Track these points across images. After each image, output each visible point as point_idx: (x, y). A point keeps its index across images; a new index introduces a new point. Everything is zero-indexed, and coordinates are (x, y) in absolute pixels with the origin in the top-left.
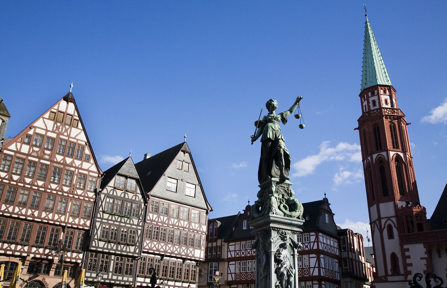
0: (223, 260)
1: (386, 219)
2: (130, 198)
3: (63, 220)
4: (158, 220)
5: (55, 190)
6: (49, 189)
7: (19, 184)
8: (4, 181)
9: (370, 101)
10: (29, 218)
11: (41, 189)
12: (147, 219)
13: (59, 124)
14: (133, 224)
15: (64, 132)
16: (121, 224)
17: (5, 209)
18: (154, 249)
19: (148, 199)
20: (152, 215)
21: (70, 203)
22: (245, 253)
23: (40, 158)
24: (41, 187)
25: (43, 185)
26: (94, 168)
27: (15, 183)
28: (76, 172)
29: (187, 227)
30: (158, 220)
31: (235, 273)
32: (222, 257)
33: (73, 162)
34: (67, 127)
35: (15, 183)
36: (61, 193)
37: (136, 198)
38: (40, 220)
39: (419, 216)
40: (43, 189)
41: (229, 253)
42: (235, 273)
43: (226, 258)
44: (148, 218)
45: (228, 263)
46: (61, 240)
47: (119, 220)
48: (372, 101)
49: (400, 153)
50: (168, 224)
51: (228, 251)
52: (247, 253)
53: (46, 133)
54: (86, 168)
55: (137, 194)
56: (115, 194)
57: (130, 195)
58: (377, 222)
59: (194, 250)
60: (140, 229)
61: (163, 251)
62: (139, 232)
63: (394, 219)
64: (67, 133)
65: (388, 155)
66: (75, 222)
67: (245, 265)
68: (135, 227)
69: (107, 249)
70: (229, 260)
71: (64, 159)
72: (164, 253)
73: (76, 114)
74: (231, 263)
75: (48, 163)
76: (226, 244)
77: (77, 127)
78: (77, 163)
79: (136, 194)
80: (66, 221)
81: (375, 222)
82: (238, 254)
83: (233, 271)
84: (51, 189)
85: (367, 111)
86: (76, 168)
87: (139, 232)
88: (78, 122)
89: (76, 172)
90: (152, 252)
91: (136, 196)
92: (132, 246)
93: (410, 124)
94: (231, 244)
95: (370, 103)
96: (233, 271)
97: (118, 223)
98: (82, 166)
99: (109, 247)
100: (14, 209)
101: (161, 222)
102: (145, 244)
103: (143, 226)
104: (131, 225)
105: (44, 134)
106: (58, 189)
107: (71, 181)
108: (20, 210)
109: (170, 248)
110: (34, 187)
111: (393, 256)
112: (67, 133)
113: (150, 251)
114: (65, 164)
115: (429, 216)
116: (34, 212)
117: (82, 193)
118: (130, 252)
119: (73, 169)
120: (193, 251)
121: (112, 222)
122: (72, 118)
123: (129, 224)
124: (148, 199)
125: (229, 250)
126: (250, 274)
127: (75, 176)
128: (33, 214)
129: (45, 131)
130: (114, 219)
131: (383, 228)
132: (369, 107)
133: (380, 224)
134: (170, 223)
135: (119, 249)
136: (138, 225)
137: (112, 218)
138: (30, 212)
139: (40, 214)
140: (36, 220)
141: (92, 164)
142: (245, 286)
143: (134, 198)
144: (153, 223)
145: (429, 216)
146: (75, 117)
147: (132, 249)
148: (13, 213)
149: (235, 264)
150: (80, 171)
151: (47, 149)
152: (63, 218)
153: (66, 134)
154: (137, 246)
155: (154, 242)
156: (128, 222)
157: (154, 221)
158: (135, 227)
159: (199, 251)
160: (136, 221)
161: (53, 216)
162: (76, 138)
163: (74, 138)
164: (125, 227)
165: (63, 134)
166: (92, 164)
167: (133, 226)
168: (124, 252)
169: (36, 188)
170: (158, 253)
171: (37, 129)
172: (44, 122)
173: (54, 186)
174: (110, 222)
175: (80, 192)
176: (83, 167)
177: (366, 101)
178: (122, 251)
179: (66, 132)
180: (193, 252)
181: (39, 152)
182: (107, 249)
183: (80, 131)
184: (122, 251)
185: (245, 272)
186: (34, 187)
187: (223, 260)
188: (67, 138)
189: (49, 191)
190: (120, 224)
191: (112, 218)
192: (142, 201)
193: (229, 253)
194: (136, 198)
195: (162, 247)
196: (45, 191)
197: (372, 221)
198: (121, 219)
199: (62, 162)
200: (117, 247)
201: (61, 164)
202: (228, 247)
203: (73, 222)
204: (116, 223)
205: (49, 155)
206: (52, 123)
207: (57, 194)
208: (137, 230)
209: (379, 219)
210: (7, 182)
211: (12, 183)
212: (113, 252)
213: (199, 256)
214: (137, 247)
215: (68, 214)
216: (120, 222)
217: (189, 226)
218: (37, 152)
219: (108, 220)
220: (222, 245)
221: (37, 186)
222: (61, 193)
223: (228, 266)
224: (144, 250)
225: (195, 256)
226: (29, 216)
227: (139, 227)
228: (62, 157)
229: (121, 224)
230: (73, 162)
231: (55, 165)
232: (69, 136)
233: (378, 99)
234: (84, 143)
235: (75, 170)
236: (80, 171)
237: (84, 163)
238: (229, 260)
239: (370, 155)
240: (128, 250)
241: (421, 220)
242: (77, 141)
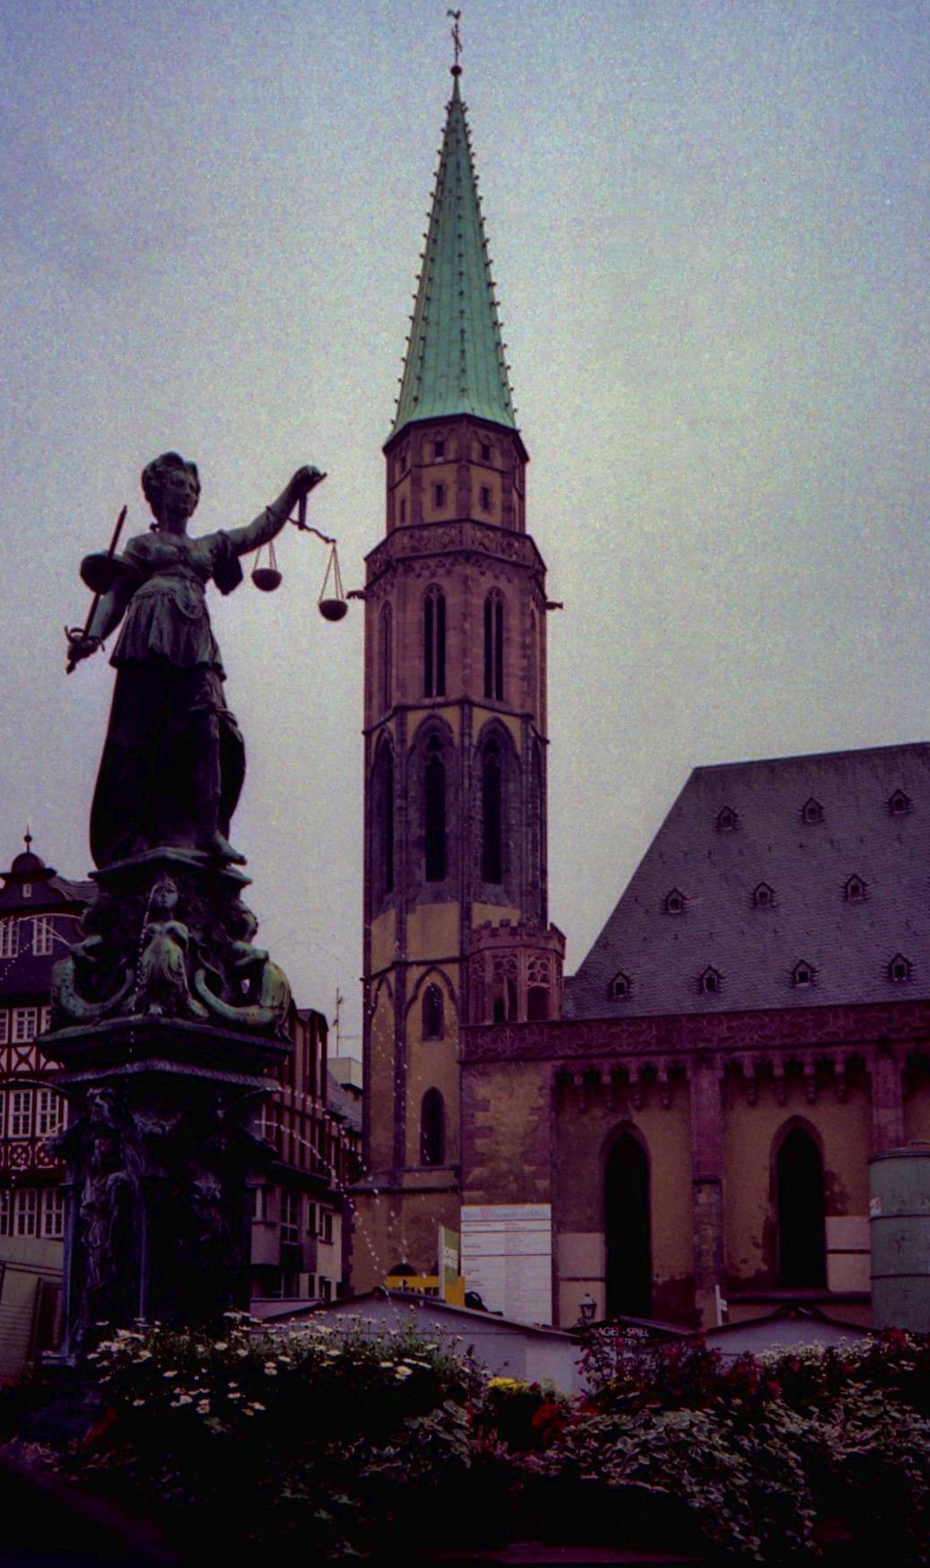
1: (422, 969)
9: (426, 483)
39: (539, 962)
48: (433, 483)
49: (505, 719)
58: (392, 977)
63: (453, 971)
65: (466, 721)
81: (382, 975)
85: (407, 523)
93: (560, 606)
95: (423, 490)
111: (433, 1100)
115: (571, 967)
131: (408, 997)
132: (418, 505)
133: (401, 981)
145: (571, 967)
177: (408, 481)
197: (374, 972)
209: (401, 966)
233: (455, 482)
239: (399, 714)
241: (544, 979)
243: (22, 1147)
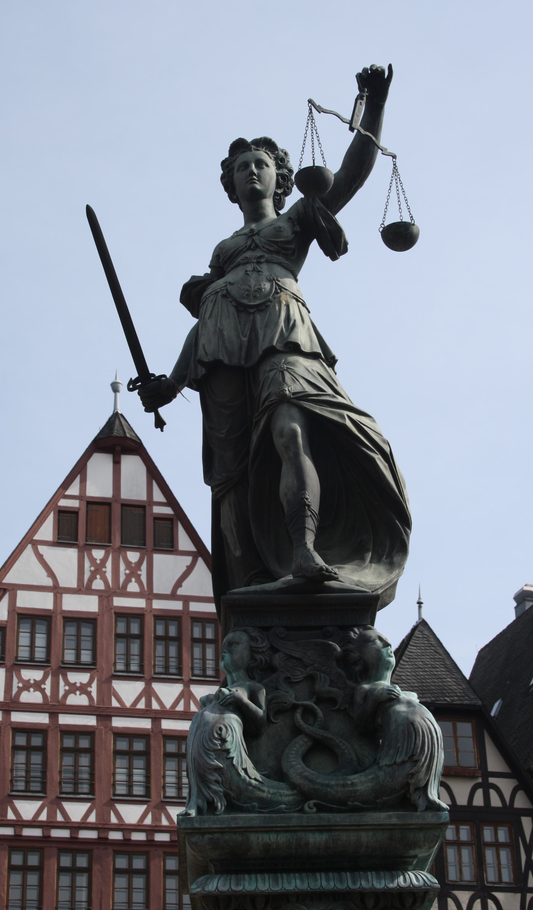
5: (138, 828)
13: (98, 554)
15: (128, 580)
34: (133, 556)
37: (487, 798)
53: (57, 601)
55: (492, 780)
73: (158, 496)
75: (91, 721)
77: (172, 546)
79: (485, 780)
88: (172, 524)
91: (486, 787)
105: (50, 606)
110: (56, 833)
122: (145, 515)
129: (50, 596)
143: (478, 800)
146: (157, 510)
153: (133, 587)
162: (180, 592)
163: (173, 596)
169: (65, 834)
171: (20, 593)
172: (40, 558)
179: (133, 580)
183: (188, 560)
188: (140, 603)
189: (115, 836)
194: (487, 798)
199: (180, 707)
206: (72, 553)
231: (118, 723)
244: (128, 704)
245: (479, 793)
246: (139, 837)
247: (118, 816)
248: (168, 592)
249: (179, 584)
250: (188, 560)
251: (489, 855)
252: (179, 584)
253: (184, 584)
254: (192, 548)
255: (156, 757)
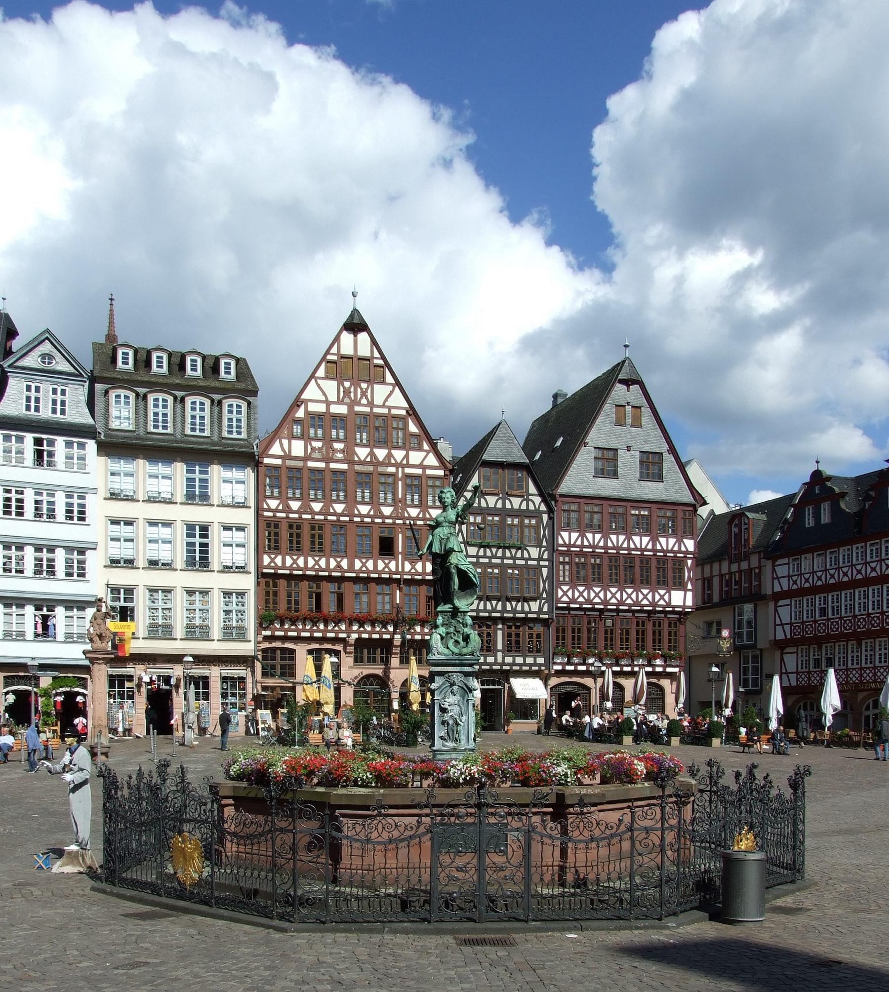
0: (764, 598)
2: (516, 507)
3: (393, 568)
4: (582, 541)
5: (368, 516)
6: (357, 516)
7: (304, 516)
8: (279, 515)
10: (334, 574)
11: (342, 519)
12: (558, 543)
14: (530, 559)
16: (506, 561)
17: (292, 564)
18: (581, 599)
19: (553, 503)
20: (567, 534)
21: (400, 535)
22: (823, 578)
23: (328, 460)
24: (342, 515)
25: (343, 511)
26: (432, 460)
27: (296, 516)
28: (400, 475)
29: (650, 547)
30: (582, 541)
31: (791, 624)
32: (763, 592)
33: (389, 455)
35: (296, 516)
36: (379, 520)
37: (528, 505)
38: (354, 575)
40: (347, 519)
41: (776, 581)
42: (791, 624)
43: (769, 592)
44: (561, 542)
45: (776, 604)
46: (397, 604)
47: (500, 554)
50: (605, 547)
51: (773, 579)
52: (816, 579)
54: (418, 463)
56: (483, 504)
57: (516, 502)
59: (669, 591)
60: (545, 566)
61: (600, 601)
62: (545, 571)
64: (367, 398)
66: (416, 570)
67: (812, 606)
68: (535, 563)
69: (485, 610)
70: (777, 597)
71: (372, 454)
72: (602, 607)
74: (781, 603)
75: (344, 466)
76: (769, 564)
78: (399, 455)
80: (400, 570)
82: (795, 582)
83: (786, 620)
84: (360, 515)
86: (397, 465)
87: (545, 571)
89: (400, 475)
90: (578, 606)
91: (528, 500)
92: (534, 599)
94: (779, 562)
96: (786, 620)
97: (499, 561)
98: (408, 461)
99: (489, 607)
100: (306, 563)
101: (589, 546)
102: (560, 593)
103: (550, 560)
104: (526, 560)
106: (372, 513)
107: (395, 494)
108: (317, 563)
109: (614, 595)
110: (330, 518)
112: (367, 398)
113: (572, 606)
114: (375, 462)
116: (341, 561)
117: (419, 514)
118: (531, 612)
119: (392, 470)
120: (667, 594)
121: (487, 560)
123: (522, 558)
124: (553, 503)
125: (775, 576)
126: (824, 624)
127: (400, 483)
128: (339, 565)
130: (489, 553)
134: (610, 544)
135: (509, 608)
136: (540, 559)
137: (485, 552)
138: (333, 564)
139: (351, 565)
140: (347, 574)
141: (428, 452)
142: (814, 648)
143: (524, 507)
144: (572, 549)
147: (534, 606)
148: (306, 568)
149: (790, 605)
150: (407, 471)
151: (338, 440)
152: (392, 565)
153: (364, 401)
154: (544, 599)
155: (578, 587)
156: (519, 555)
157: (574, 546)
158: (535, 563)
159: (682, 593)
160: (534, 552)
161: (375, 565)
162: (387, 404)
163: (383, 406)
164: (514, 566)
165: (359, 404)
166: (428, 452)
167: (530, 562)
168: (519, 612)
169: (334, 518)
170: (590, 606)
173: (364, 509)
174: (481, 560)
175: (414, 512)
176: (411, 462)
178: (514, 611)
180: (666, 597)
181: (324, 450)
182: (485, 610)
183: (391, 388)
184: (514, 611)
185: (813, 619)
186: (330, 518)
187: (764, 598)
188: (368, 409)
190: (502, 561)
191: (485, 552)
192: (543, 508)
193: (776, 581)
194: (528, 505)
195: (597, 595)
196: (351, 521)
198: (504, 553)
200: (504, 606)
201: (370, 464)
202: (774, 570)
203: (413, 571)
204: (494, 561)
205: (342, 451)
207: (373, 522)
208: (539, 567)
210: (284, 515)
211: (291, 515)
212: (499, 615)
213: (681, 604)
214: (543, 601)
215: (400, 556)
216: (503, 557)
217: (654, 545)
218: (320, 449)
219: (477, 557)
220: (760, 567)
221: (335, 514)
222: (379, 520)
223: (776, 610)
224: (559, 605)
225: (673, 603)
226: (334, 570)
227: (542, 563)
228: (368, 450)
229: (506, 561)
230: (389, 455)
231: (358, 468)
232: (371, 404)
234: (404, 412)
235: (397, 470)
236: (407, 471)
237: (411, 453)
238: (777, 597)
240: (526, 609)
242: (390, 411)
243: (863, 618)
244: (362, 459)
245: (525, 503)
246: (368, 520)
247: (358, 510)
248: (381, 404)
249: (386, 400)
250: (391, 388)
251: (526, 530)
252: (386, 400)
253: (389, 400)
254: (393, 382)
255: (375, 485)
